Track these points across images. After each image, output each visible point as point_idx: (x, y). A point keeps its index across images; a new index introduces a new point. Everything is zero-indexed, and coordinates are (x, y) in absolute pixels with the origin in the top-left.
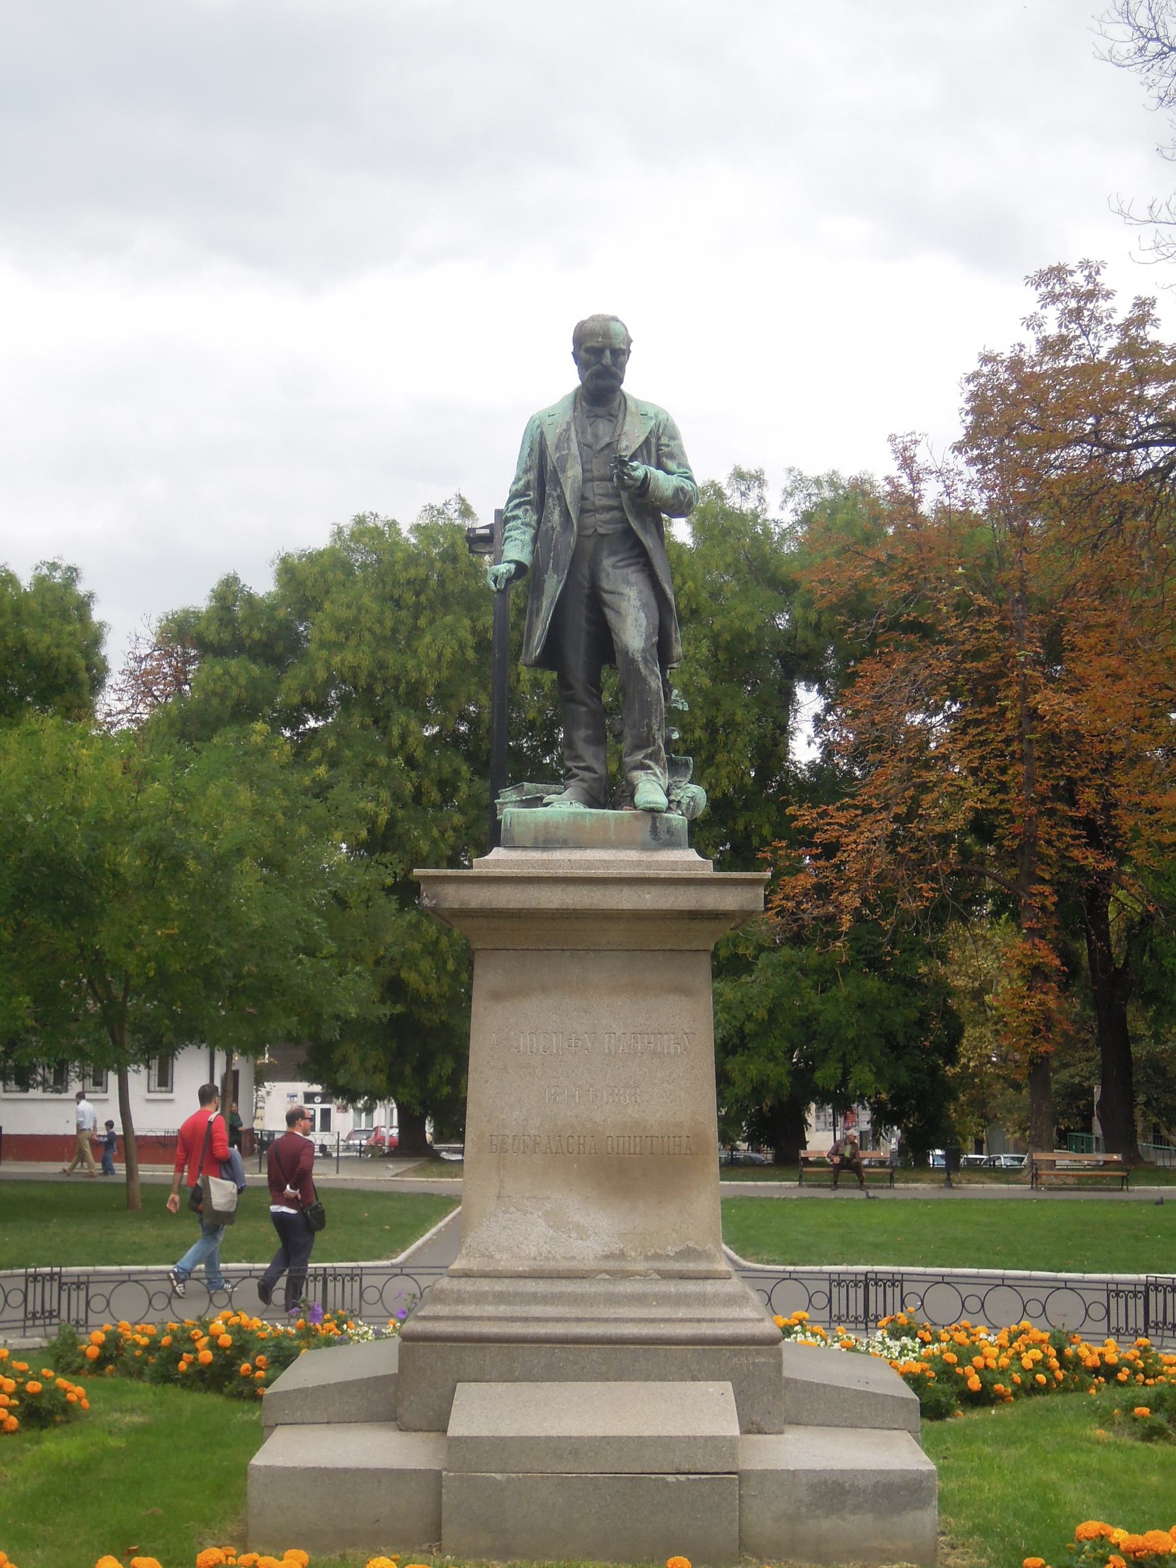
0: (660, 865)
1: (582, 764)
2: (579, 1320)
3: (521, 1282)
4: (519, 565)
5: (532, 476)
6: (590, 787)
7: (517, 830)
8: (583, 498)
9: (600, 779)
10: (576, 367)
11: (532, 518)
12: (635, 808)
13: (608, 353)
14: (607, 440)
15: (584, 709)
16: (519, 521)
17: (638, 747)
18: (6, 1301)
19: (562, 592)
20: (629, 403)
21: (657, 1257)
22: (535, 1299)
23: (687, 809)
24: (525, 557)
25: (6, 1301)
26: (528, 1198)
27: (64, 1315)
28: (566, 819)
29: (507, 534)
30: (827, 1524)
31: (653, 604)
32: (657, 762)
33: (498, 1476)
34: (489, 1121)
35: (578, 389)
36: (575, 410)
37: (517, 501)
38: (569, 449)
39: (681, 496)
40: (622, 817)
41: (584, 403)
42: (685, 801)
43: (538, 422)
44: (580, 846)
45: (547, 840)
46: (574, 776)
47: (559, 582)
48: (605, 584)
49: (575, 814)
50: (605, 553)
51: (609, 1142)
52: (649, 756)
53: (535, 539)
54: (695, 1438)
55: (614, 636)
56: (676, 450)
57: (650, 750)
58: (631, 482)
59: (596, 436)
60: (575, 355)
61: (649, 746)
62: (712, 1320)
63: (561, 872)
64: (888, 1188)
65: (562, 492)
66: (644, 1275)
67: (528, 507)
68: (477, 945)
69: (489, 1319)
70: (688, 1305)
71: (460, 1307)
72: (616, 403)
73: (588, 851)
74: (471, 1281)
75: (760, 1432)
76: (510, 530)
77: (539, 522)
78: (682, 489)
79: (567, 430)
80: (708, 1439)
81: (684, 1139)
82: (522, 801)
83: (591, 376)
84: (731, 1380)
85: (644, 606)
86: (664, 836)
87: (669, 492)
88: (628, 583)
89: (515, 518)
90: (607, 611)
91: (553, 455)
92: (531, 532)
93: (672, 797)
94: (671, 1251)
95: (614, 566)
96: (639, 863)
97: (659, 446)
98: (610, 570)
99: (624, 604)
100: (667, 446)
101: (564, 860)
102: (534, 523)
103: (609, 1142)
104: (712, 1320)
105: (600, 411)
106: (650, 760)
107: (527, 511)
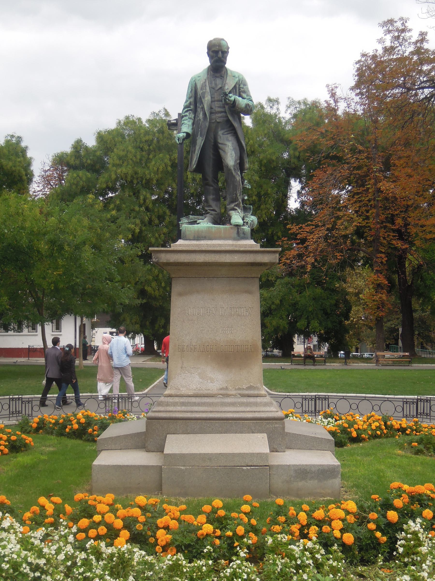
0: (240, 246)
1: (211, 209)
2: (211, 412)
3: (190, 398)
4: (188, 134)
5: (192, 100)
6: (214, 217)
7: (187, 233)
8: (211, 108)
9: (218, 214)
10: (208, 58)
11: (192, 116)
12: (231, 225)
13: (220, 53)
14: (220, 86)
15: (212, 188)
16: (187, 117)
17: (232, 202)
18: (2, 408)
19: (203, 144)
20: (228, 72)
21: (239, 389)
22: (195, 404)
23: (250, 225)
24: (189, 131)
25: (2, 408)
26: (192, 368)
27: (24, 413)
28: (205, 229)
29: (183, 122)
30: (301, 484)
31: (237, 148)
32: (239, 207)
33: (182, 468)
34: (178, 340)
35: (209, 66)
36: (208, 74)
37: (186, 109)
38: (206, 89)
39: (248, 107)
40: (226, 228)
41: (211, 72)
42: (249, 222)
43: (194, 79)
44: (210, 239)
45: (198, 237)
46: (208, 213)
47: (202, 140)
48: (220, 141)
49: (209, 227)
50: (219, 129)
51: (222, 348)
52: (236, 205)
53: (193, 124)
54: (253, 453)
55: (223, 161)
56: (246, 90)
57: (236, 203)
58: (229, 102)
59: (216, 84)
60: (208, 53)
61: (236, 202)
62: (259, 412)
63: (204, 249)
64: (323, 365)
65: (203, 106)
66: (235, 396)
67: (191, 112)
68: (173, 276)
69: (178, 411)
70: (251, 406)
71: (168, 408)
72: (223, 72)
73: (214, 241)
74: (172, 398)
75: (277, 452)
76: (184, 120)
77: (195, 117)
78: (248, 104)
79: (205, 82)
80: (258, 454)
81: (249, 346)
82: (189, 222)
83: (214, 62)
84: (266, 433)
85: (234, 149)
86: (242, 235)
87: (244, 106)
88: (228, 140)
89: (186, 116)
90: (220, 151)
91: (200, 92)
92: (191, 121)
93: (245, 221)
94: (244, 387)
95: (223, 134)
96: (232, 245)
97: (239, 88)
98: (221, 135)
99: (227, 148)
100: (243, 88)
101: (205, 244)
102: (193, 118)
103: (222, 348)
104: (259, 412)
105: (218, 75)
106: (237, 206)
107: (190, 113)
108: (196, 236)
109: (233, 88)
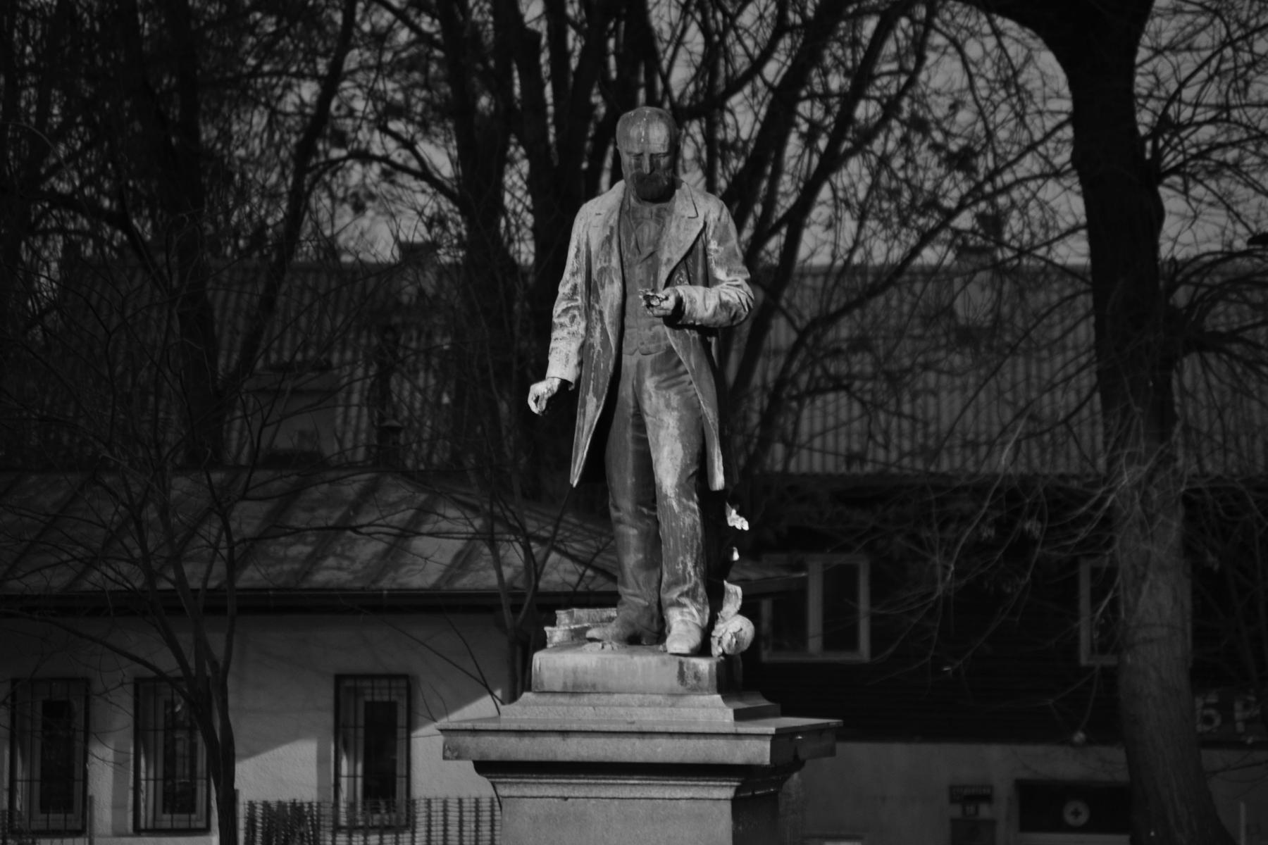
7: (546, 675)
16: (566, 331)
47: (598, 407)
61: (685, 582)
86: (691, 681)
92: (574, 346)
108: (570, 684)
109: (685, 258)
